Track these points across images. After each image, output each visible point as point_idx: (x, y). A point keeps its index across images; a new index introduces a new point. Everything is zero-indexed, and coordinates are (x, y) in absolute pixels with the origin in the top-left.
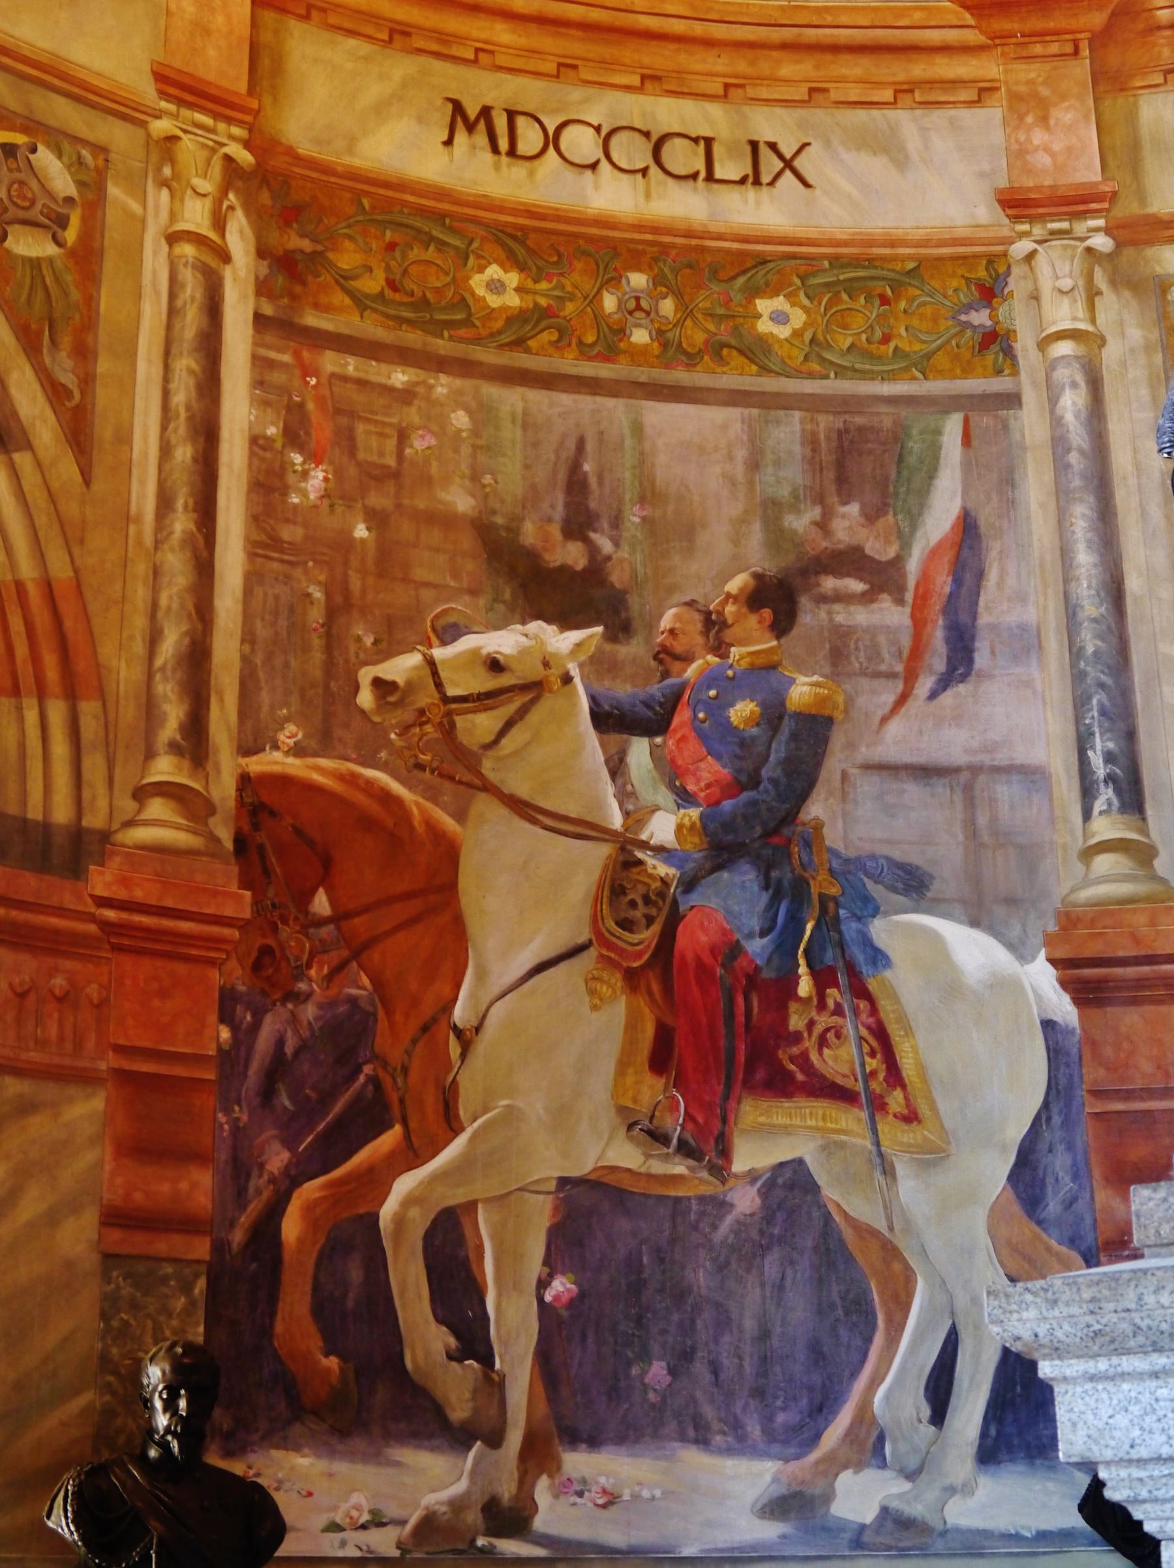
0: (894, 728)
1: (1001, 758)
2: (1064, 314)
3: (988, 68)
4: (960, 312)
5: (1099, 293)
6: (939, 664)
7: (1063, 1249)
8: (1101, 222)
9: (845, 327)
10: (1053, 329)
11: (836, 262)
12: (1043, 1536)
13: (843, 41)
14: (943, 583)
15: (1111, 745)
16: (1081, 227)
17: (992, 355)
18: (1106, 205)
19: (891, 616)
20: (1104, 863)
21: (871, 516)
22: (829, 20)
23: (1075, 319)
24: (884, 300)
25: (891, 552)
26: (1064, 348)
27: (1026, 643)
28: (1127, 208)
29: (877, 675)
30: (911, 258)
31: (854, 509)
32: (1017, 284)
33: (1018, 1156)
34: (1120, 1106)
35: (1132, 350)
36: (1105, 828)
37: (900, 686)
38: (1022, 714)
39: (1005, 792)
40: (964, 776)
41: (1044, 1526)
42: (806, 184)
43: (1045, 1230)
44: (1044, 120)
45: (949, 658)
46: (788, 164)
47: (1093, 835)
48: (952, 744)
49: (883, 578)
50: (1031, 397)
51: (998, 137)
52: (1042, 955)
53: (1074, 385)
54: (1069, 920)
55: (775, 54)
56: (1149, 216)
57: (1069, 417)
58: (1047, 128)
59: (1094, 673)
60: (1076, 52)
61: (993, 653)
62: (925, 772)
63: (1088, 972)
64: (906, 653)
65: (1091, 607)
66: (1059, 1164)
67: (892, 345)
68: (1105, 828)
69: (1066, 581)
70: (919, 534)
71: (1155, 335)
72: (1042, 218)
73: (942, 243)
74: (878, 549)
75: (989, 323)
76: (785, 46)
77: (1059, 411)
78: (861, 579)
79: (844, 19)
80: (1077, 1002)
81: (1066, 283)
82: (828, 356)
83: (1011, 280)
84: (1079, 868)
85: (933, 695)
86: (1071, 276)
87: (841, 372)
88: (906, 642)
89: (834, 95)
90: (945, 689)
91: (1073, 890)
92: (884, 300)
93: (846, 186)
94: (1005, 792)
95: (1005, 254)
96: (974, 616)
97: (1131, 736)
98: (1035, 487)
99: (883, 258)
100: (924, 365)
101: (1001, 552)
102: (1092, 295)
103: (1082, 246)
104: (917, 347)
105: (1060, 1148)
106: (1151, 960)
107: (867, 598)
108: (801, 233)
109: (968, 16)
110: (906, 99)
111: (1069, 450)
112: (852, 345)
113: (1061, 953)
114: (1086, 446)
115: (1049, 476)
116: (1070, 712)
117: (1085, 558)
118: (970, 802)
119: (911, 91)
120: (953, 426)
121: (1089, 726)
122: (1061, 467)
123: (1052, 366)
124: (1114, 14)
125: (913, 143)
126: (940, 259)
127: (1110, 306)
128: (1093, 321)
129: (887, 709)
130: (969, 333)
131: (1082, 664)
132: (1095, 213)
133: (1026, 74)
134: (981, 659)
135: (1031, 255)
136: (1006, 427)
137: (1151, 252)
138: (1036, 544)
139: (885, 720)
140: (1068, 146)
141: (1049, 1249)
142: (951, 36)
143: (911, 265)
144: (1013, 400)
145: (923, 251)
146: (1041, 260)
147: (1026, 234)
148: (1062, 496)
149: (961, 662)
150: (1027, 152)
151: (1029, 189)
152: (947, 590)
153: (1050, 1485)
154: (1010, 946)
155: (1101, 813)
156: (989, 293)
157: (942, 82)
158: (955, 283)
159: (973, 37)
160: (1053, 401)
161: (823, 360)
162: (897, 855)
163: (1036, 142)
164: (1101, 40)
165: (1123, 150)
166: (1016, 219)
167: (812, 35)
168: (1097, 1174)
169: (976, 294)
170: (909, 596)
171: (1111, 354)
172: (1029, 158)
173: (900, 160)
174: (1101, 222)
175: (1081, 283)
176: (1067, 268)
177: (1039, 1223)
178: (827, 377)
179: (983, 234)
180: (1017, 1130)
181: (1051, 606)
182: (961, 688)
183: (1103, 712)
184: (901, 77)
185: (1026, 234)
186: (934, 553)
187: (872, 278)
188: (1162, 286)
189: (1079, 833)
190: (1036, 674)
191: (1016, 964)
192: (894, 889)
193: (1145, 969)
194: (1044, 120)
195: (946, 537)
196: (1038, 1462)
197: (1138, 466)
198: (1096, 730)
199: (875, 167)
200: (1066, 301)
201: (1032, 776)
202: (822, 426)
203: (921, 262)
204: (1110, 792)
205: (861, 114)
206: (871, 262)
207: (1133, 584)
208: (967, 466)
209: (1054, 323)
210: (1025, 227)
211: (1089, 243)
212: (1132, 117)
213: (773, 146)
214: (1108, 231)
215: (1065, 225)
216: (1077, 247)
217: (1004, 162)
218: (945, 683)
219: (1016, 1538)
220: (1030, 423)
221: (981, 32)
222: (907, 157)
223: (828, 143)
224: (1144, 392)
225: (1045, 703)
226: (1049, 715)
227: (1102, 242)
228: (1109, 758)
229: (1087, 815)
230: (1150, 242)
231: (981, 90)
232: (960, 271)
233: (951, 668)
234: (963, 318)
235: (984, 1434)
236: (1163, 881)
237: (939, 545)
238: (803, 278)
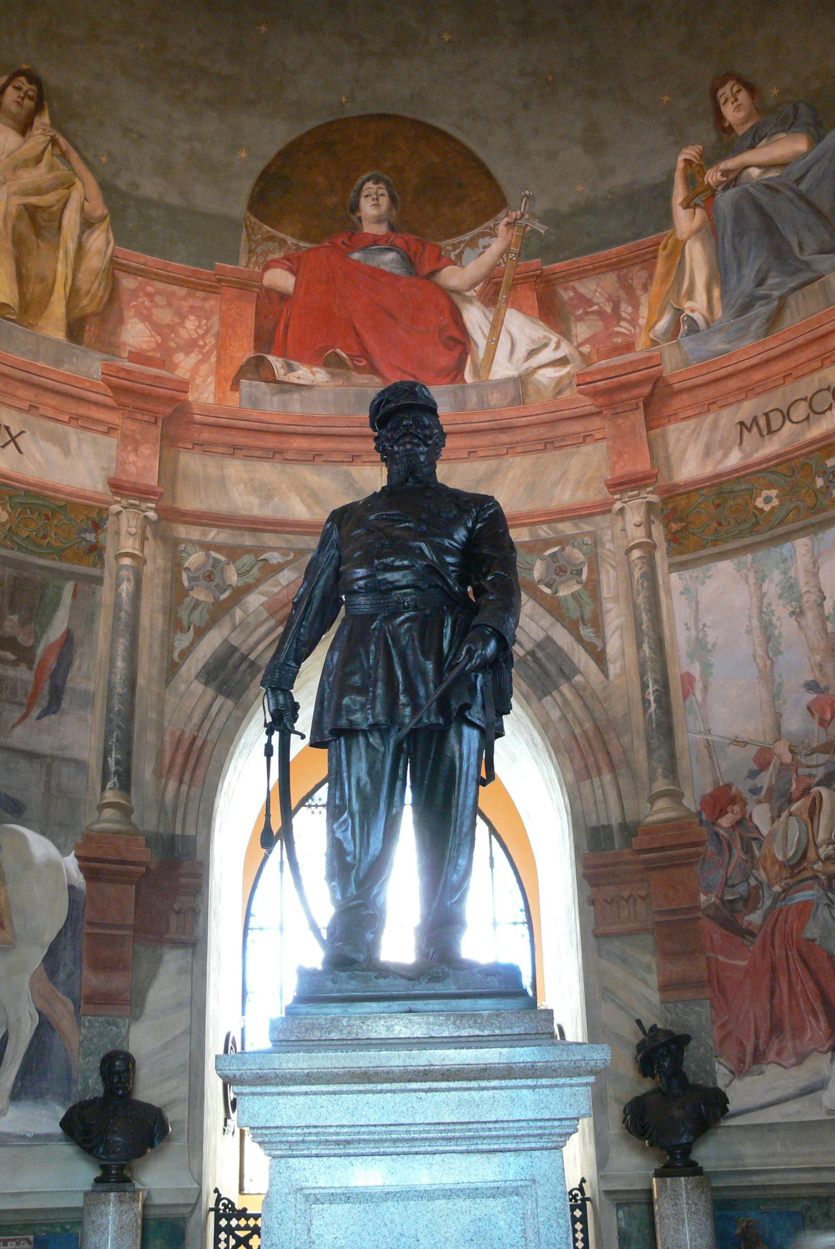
0: (19, 731)
1: (67, 754)
2: (129, 545)
3: (115, 418)
4: (82, 532)
5: (147, 539)
6: (44, 703)
7: (64, 998)
8: (153, 505)
9: (26, 526)
10: (123, 551)
11: (27, 493)
12: (37, 1137)
13: (50, 386)
14: (52, 663)
15: (119, 756)
16: (144, 506)
17: (93, 557)
18: (157, 498)
19: (25, 674)
20: (108, 813)
21: (23, 623)
22: (45, 374)
23: (134, 548)
24: (47, 518)
25: (30, 643)
26: (127, 561)
27: (87, 700)
28: (166, 502)
29: (14, 703)
30: (62, 500)
31: (15, 618)
32: (110, 525)
33: (49, 951)
34: (100, 931)
35: (158, 570)
36: (110, 796)
37: (24, 710)
38: (79, 735)
39: (66, 770)
40: (48, 760)
41: (37, 1132)
42: (20, 452)
43: (57, 988)
44: (136, 450)
45: (49, 703)
46: (13, 439)
47: (105, 798)
48: (45, 743)
49: (25, 655)
50: (107, 580)
51: (113, 452)
52: (73, 853)
53: (128, 580)
54: (88, 838)
55: (16, 383)
56: (174, 508)
57: (124, 595)
58: (137, 454)
59: (117, 720)
60: (156, 423)
61: (70, 702)
62: (31, 756)
63: (92, 864)
64: (29, 695)
65: (119, 690)
66: (67, 955)
67: (47, 540)
68: (110, 796)
69: (110, 673)
70: (45, 636)
71: (169, 565)
72: (127, 497)
73: (79, 497)
74: (25, 640)
75: (94, 541)
76: (22, 381)
77: (120, 591)
78: (13, 653)
79: (52, 376)
80: (86, 878)
81: (133, 530)
82: (15, 538)
83: (108, 522)
84: (96, 813)
85: (39, 718)
86: (136, 527)
87: (21, 548)
88: (30, 689)
89: (40, 411)
90: (45, 715)
91: (91, 824)
92: (47, 518)
93: (38, 457)
94: (66, 771)
95: (107, 510)
96: (64, 683)
97: (129, 754)
98: (103, 625)
99: (50, 497)
100: (60, 553)
101: (81, 654)
102: (144, 539)
103: (143, 514)
104: (58, 544)
105: (69, 948)
106: (123, 862)
107: (15, 664)
108: (13, 474)
109: (110, 391)
110: (74, 422)
111: (121, 611)
112: (28, 536)
113: (81, 854)
114: (129, 610)
115: (110, 621)
116: (103, 738)
117: (120, 664)
118: (49, 773)
119: (78, 419)
120: (69, 587)
121: (111, 746)
122: (116, 618)
123: (120, 568)
124: (175, 410)
125: (74, 445)
126: (77, 504)
127: (151, 546)
128: (142, 551)
129: (16, 720)
130: (84, 543)
131: (112, 715)
132: (152, 501)
133: (131, 426)
134: (64, 704)
135: (119, 513)
136: (94, 593)
137: (174, 525)
138: (99, 654)
139: (14, 726)
140: (144, 466)
141: (57, 996)
142: (101, 398)
143: (63, 504)
144: (99, 581)
145: (69, 498)
146: (124, 517)
147: (119, 502)
148: (114, 631)
149: (54, 705)
150: (125, 463)
151: (124, 481)
152: (54, 667)
153: (43, 1112)
154: (59, 847)
155: (110, 789)
156: (97, 527)
157: (93, 419)
158: (82, 517)
159: (109, 401)
160: (118, 585)
161: (13, 541)
162: (10, 794)
163: (130, 460)
164: (168, 420)
165: (169, 473)
166: (116, 494)
167: (36, 379)
168: (85, 962)
169: (90, 525)
170: (35, 666)
171: (148, 569)
172: (126, 466)
173: (66, 451)
174: (153, 505)
175: (140, 532)
176: (135, 523)
177: (54, 984)
178: (13, 549)
179: (98, 497)
180: (49, 937)
181: (102, 683)
182: (53, 716)
183: (117, 741)
184: (74, 411)
185: (119, 502)
186: (49, 648)
187: (43, 505)
188: (177, 542)
189: (98, 797)
190: (89, 716)
191: (60, 856)
192: (6, 811)
193: (120, 867)
194: (136, 450)
195: (57, 641)
196: (39, 1100)
197: (152, 625)
198: (113, 748)
199: (54, 452)
200: (131, 539)
201: (80, 765)
202: (7, 573)
203: (68, 503)
204: (116, 779)
205: (52, 425)
206: (45, 497)
207: (141, 681)
208: (73, 608)
209: (124, 548)
210: (119, 499)
211: (146, 513)
212: (175, 461)
213: (7, 428)
214: (156, 510)
215: (137, 502)
216: (139, 514)
217: (114, 465)
218: (45, 713)
219: (23, 1137)
220: (106, 593)
221: (115, 401)
222: (70, 450)
223: (33, 434)
224: (160, 591)
225: (91, 731)
226: (93, 736)
227: (152, 515)
228: (117, 763)
229: (103, 789)
230: (174, 521)
231: (109, 428)
232: (85, 512)
233: (50, 705)
234: (83, 535)
235: (14, 1086)
236: (135, 826)
237: (53, 644)
238: (10, 497)
